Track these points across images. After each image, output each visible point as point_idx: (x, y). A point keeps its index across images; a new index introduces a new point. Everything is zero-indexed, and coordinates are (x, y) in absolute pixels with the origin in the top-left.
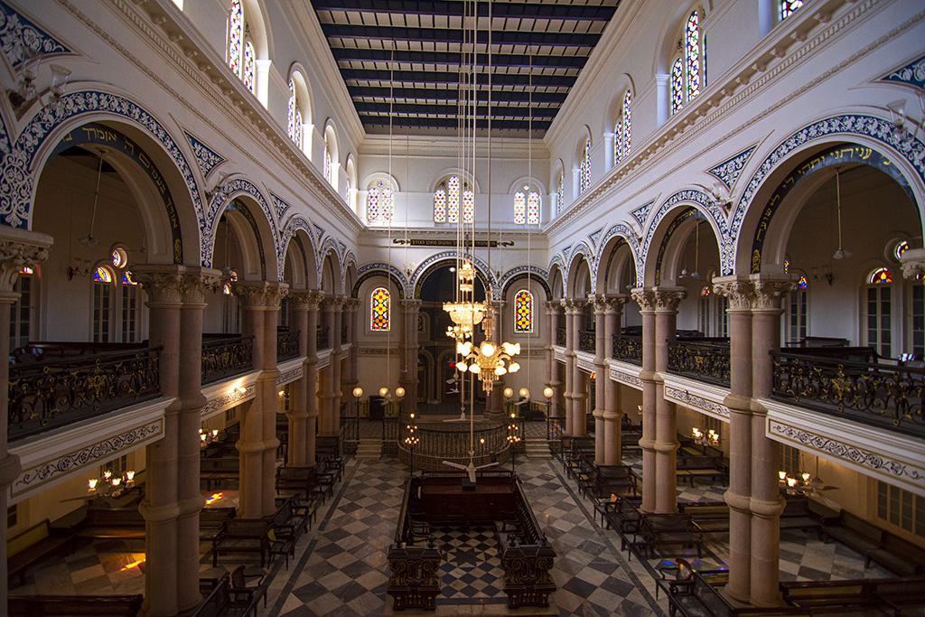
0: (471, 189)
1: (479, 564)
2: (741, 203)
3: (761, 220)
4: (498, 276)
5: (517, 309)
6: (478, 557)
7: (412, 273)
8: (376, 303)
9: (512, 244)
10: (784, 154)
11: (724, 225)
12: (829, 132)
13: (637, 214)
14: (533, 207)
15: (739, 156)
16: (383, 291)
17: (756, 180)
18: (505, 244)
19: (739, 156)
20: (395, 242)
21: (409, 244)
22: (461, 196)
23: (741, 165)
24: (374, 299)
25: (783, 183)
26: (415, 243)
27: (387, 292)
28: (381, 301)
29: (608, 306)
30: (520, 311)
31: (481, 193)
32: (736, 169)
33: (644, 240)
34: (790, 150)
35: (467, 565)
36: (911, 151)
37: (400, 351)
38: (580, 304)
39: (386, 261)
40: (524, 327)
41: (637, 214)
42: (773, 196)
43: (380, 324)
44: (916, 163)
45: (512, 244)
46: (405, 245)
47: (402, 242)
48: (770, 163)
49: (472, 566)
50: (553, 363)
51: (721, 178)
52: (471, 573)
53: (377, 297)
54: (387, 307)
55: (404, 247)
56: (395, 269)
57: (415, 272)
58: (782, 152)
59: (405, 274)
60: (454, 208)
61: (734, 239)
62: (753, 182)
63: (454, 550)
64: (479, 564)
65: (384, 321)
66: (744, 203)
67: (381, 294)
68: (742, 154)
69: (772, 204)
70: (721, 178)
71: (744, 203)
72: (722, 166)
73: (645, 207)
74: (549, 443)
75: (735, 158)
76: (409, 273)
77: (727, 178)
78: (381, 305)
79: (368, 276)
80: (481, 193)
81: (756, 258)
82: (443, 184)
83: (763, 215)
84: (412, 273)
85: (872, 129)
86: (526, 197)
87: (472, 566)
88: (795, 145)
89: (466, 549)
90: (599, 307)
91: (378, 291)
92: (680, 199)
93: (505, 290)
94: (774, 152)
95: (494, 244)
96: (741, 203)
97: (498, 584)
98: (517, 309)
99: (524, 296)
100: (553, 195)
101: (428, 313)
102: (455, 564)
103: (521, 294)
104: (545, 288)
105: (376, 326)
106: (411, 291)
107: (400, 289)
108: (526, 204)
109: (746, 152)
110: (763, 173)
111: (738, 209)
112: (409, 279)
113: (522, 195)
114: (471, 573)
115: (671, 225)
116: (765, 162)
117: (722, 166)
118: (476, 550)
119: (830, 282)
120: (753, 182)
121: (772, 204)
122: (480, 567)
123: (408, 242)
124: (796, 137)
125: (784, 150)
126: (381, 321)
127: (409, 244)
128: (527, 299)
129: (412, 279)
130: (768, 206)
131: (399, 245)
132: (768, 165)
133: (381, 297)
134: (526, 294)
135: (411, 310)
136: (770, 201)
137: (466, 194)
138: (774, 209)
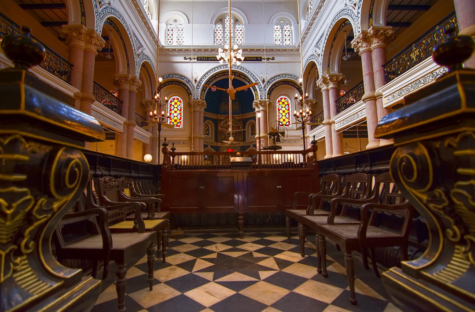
0: (241, 23)
1: (264, 275)
4: (264, 81)
5: (279, 110)
6: (262, 263)
7: (198, 80)
8: (172, 108)
9: (273, 59)
14: (287, 34)
16: (178, 99)
18: (268, 59)
20: (185, 59)
24: (171, 105)
26: (200, 59)
27: (180, 99)
28: (176, 106)
29: (375, 41)
30: (281, 112)
31: (249, 23)
35: (236, 277)
39: (178, 73)
40: (284, 123)
45: (273, 59)
49: (253, 279)
52: (245, 292)
53: (173, 103)
54: (181, 110)
55: (191, 62)
63: (214, 256)
64: (264, 275)
67: (176, 101)
76: (196, 81)
84: (198, 80)
86: (282, 28)
87: (253, 279)
89: (235, 255)
91: (174, 99)
93: (269, 94)
95: (258, 59)
98: (279, 110)
99: (283, 100)
101: (214, 123)
102: (209, 276)
106: (197, 94)
107: (190, 94)
108: (282, 33)
112: (195, 85)
113: (279, 27)
114: (245, 292)
118: (256, 255)
123: (194, 59)
127: (196, 60)
128: (286, 103)
129: (198, 85)
131: (188, 60)
135: (198, 108)
137: (237, 27)
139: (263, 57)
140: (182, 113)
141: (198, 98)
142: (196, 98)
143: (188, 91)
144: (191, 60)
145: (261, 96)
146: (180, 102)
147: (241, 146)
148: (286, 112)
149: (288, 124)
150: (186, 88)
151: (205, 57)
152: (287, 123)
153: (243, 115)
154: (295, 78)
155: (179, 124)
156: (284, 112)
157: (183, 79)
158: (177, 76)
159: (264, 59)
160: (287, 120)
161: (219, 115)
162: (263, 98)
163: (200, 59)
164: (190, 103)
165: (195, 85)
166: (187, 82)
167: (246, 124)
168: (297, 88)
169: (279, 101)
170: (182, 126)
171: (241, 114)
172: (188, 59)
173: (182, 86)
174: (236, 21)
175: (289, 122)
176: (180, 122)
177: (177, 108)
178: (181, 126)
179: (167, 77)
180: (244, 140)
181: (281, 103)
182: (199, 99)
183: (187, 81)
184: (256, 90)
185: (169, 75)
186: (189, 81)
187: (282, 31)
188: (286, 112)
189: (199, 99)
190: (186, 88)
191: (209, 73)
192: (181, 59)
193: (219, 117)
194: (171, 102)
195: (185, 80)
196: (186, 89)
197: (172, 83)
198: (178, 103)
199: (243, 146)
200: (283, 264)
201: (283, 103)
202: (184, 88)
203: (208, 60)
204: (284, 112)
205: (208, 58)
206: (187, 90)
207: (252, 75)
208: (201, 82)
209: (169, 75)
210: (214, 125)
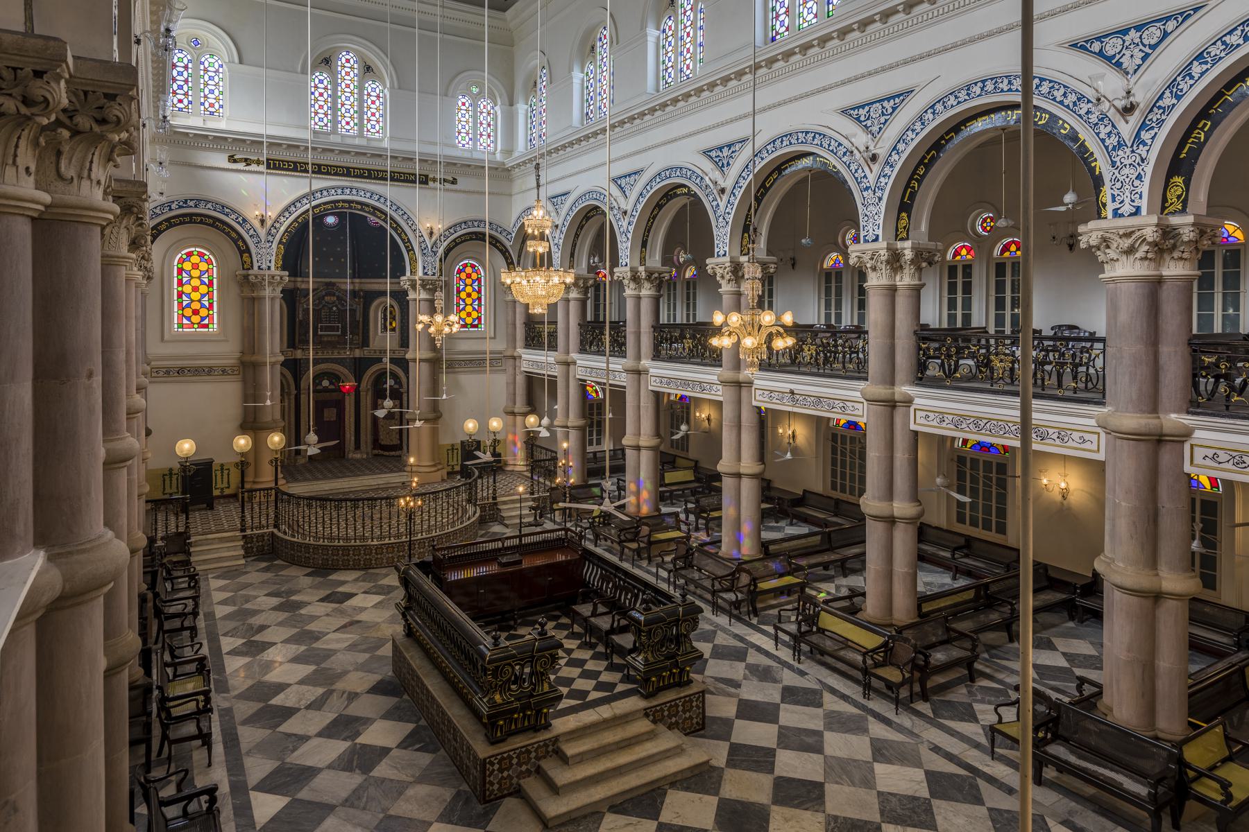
0: (379, 78)
1: (562, 662)
2: (890, 155)
3: (911, 179)
5: (459, 291)
9: (454, 182)
10: (952, 106)
11: (865, 180)
12: (1009, 90)
13: (713, 154)
15: (888, 99)
16: (201, 255)
17: (913, 130)
19: (888, 99)
21: (262, 168)
22: (361, 88)
23: (890, 110)
25: (942, 138)
26: (275, 165)
28: (196, 273)
30: (463, 295)
31: (400, 88)
32: (883, 114)
33: (728, 191)
34: (959, 103)
36: (1097, 124)
37: (248, 369)
38: (581, 283)
40: (469, 320)
41: (713, 154)
42: (928, 152)
43: (196, 319)
44: (1102, 136)
45: (454, 182)
46: (254, 167)
47: (247, 162)
48: (934, 113)
50: (520, 380)
51: (861, 122)
53: (187, 266)
54: (211, 284)
56: (234, 211)
57: (276, 221)
58: (949, 103)
59: (257, 224)
60: (348, 101)
61: (880, 199)
62: (909, 133)
65: (204, 312)
66: (895, 157)
67: (195, 259)
68: (893, 97)
69: (926, 161)
70: (861, 122)
71: (895, 157)
72: (863, 107)
73: (729, 146)
74: (534, 500)
75: (883, 100)
77: (869, 123)
78: (196, 282)
79: (171, 223)
80: (400, 88)
81: (903, 223)
82: (326, 62)
83: (914, 173)
85: (1058, 95)
86: (474, 105)
88: (967, 97)
90: (632, 285)
91: (190, 254)
92: (793, 141)
94: (939, 102)
96: (890, 155)
97: (606, 677)
98: (459, 291)
99: (469, 270)
100: (521, 108)
103: (465, 266)
104: (506, 259)
105: (185, 321)
106: (268, 258)
107: (244, 250)
109: (898, 96)
110: (923, 124)
111: (887, 163)
115: (770, 174)
116: (926, 112)
117: (863, 107)
119: (793, 265)
120: (909, 133)
121: (926, 161)
122: (566, 665)
123: (258, 162)
124: (968, 89)
125: (952, 101)
126: (196, 312)
128: (474, 276)
129: (269, 233)
130: (921, 162)
131: (241, 166)
132: (931, 117)
133: (195, 266)
134: (473, 266)
136: (924, 157)
137: (369, 86)
138: (928, 167)
139: (431, 176)
140: (215, 292)
141: (269, 268)
142: (264, 266)
143: (240, 243)
144: (248, 165)
145: (424, 268)
146: (209, 262)
147: (355, 358)
148: (475, 295)
149: (476, 323)
150: (234, 235)
151: (288, 162)
152: (474, 320)
153: (363, 280)
154: (499, 229)
155: (206, 322)
156: (469, 295)
157: (227, 215)
158: (209, 206)
159: (434, 180)
160: (475, 315)
161: (299, 279)
162: (430, 273)
163: (275, 164)
164: (246, 277)
165: (262, 232)
166: (238, 223)
167: (369, 308)
168: (501, 251)
169: (459, 272)
170: (215, 326)
171: (359, 277)
172: (240, 160)
173: (223, 231)
174: (368, 69)
175: (479, 319)
176: (210, 317)
177: (199, 278)
178: (214, 328)
179: (180, 207)
180: (365, 342)
181: (463, 276)
182: (273, 268)
183: (240, 219)
184: (413, 249)
185: (186, 200)
186: (244, 220)
187: (475, 111)
188: (475, 295)
189: (273, 268)
190: (234, 235)
191: (298, 205)
192: (220, 160)
193: (299, 285)
194: (182, 261)
195: (233, 217)
196: (232, 238)
197: (191, 219)
198: (203, 266)
199: (360, 358)
200: (569, 652)
201: (469, 276)
202: (228, 234)
203: (295, 170)
204: (469, 295)
205: (295, 163)
206: (235, 242)
207: (405, 217)
208: (277, 225)
209: (186, 200)
210: (288, 307)
